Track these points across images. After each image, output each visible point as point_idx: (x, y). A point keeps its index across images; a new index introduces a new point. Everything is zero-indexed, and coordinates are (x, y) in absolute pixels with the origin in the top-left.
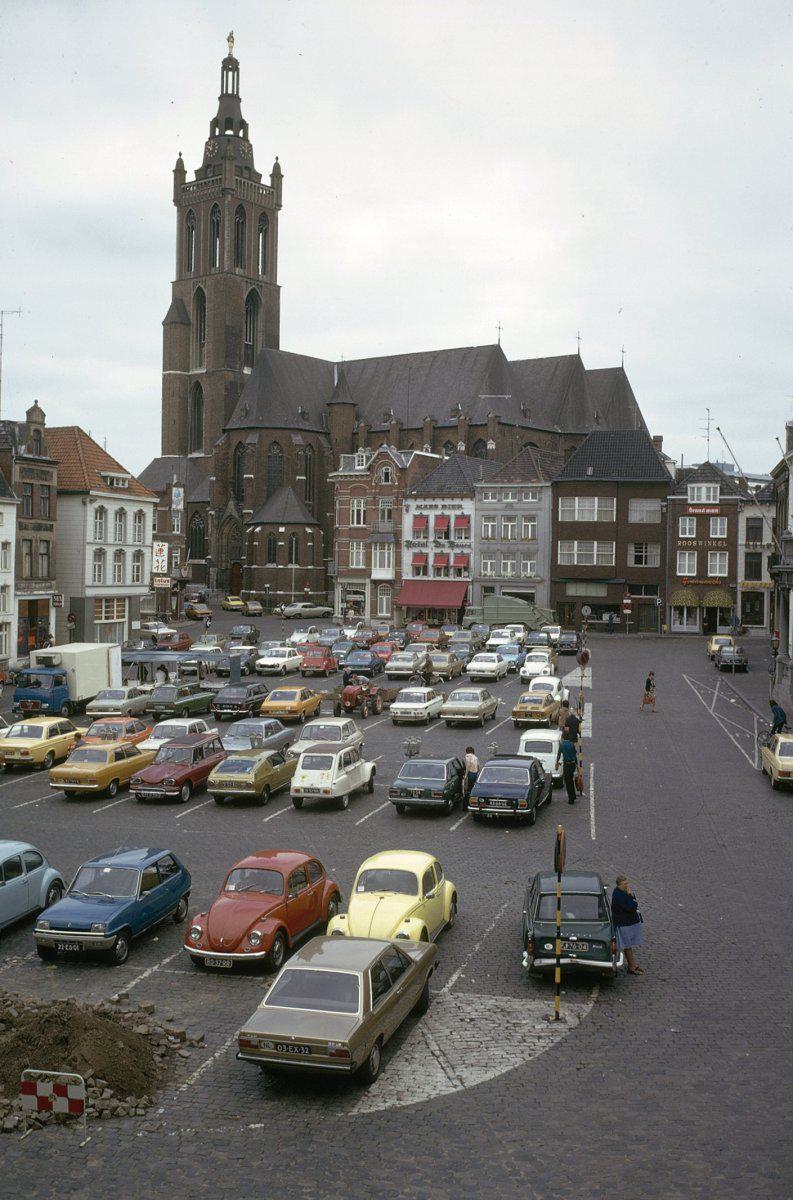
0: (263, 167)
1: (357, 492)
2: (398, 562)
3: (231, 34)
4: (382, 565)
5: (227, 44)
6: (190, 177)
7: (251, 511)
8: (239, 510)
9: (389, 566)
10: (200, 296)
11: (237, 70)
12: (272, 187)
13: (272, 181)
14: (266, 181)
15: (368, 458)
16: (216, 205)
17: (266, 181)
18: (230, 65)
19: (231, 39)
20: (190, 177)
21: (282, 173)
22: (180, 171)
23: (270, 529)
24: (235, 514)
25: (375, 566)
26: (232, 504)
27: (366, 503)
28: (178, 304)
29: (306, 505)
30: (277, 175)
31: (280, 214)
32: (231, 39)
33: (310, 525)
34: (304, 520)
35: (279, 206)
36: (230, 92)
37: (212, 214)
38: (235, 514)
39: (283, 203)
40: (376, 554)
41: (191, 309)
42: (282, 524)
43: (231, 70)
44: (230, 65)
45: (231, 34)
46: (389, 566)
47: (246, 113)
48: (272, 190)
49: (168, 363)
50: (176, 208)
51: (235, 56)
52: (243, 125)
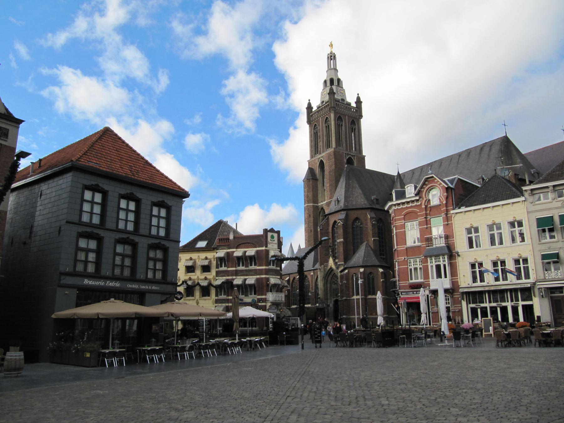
0: (351, 99)
1: (409, 216)
2: (454, 273)
3: (331, 43)
4: (439, 276)
5: (330, 48)
6: (315, 109)
7: (343, 263)
8: (336, 264)
9: (446, 277)
10: (322, 164)
11: (335, 57)
12: (357, 107)
13: (356, 105)
14: (354, 105)
15: (416, 187)
16: (327, 118)
17: (354, 105)
18: (332, 57)
19: (331, 45)
20: (315, 109)
21: (361, 100)
22: (309, 107)
23: (353, 271)
24: (334, 267)
25: (433, 278)
26: (331, 261)
27: (420, 224)
28: (311, 171)
29: (382, 258)
30: (359, 102)
31: (362, 121)
32: (331, 45)
33: (381, 267)
34: (377, 263)
35: (361, 116)
36: (332, 67)
37: (325, 123)
38: (334, 267)
39: (363, 115)
40: (432, 266)
41: (317, 171)
42: (362, 267)
43: (331, 59)
44: (332, 57)
45: (331, 43)
46: (446, 277)
47: (341, 75)
48: (356, 109)
49: (307, 200)
50: (308, 126)
51: (333, 52)
52: (339, 80)
